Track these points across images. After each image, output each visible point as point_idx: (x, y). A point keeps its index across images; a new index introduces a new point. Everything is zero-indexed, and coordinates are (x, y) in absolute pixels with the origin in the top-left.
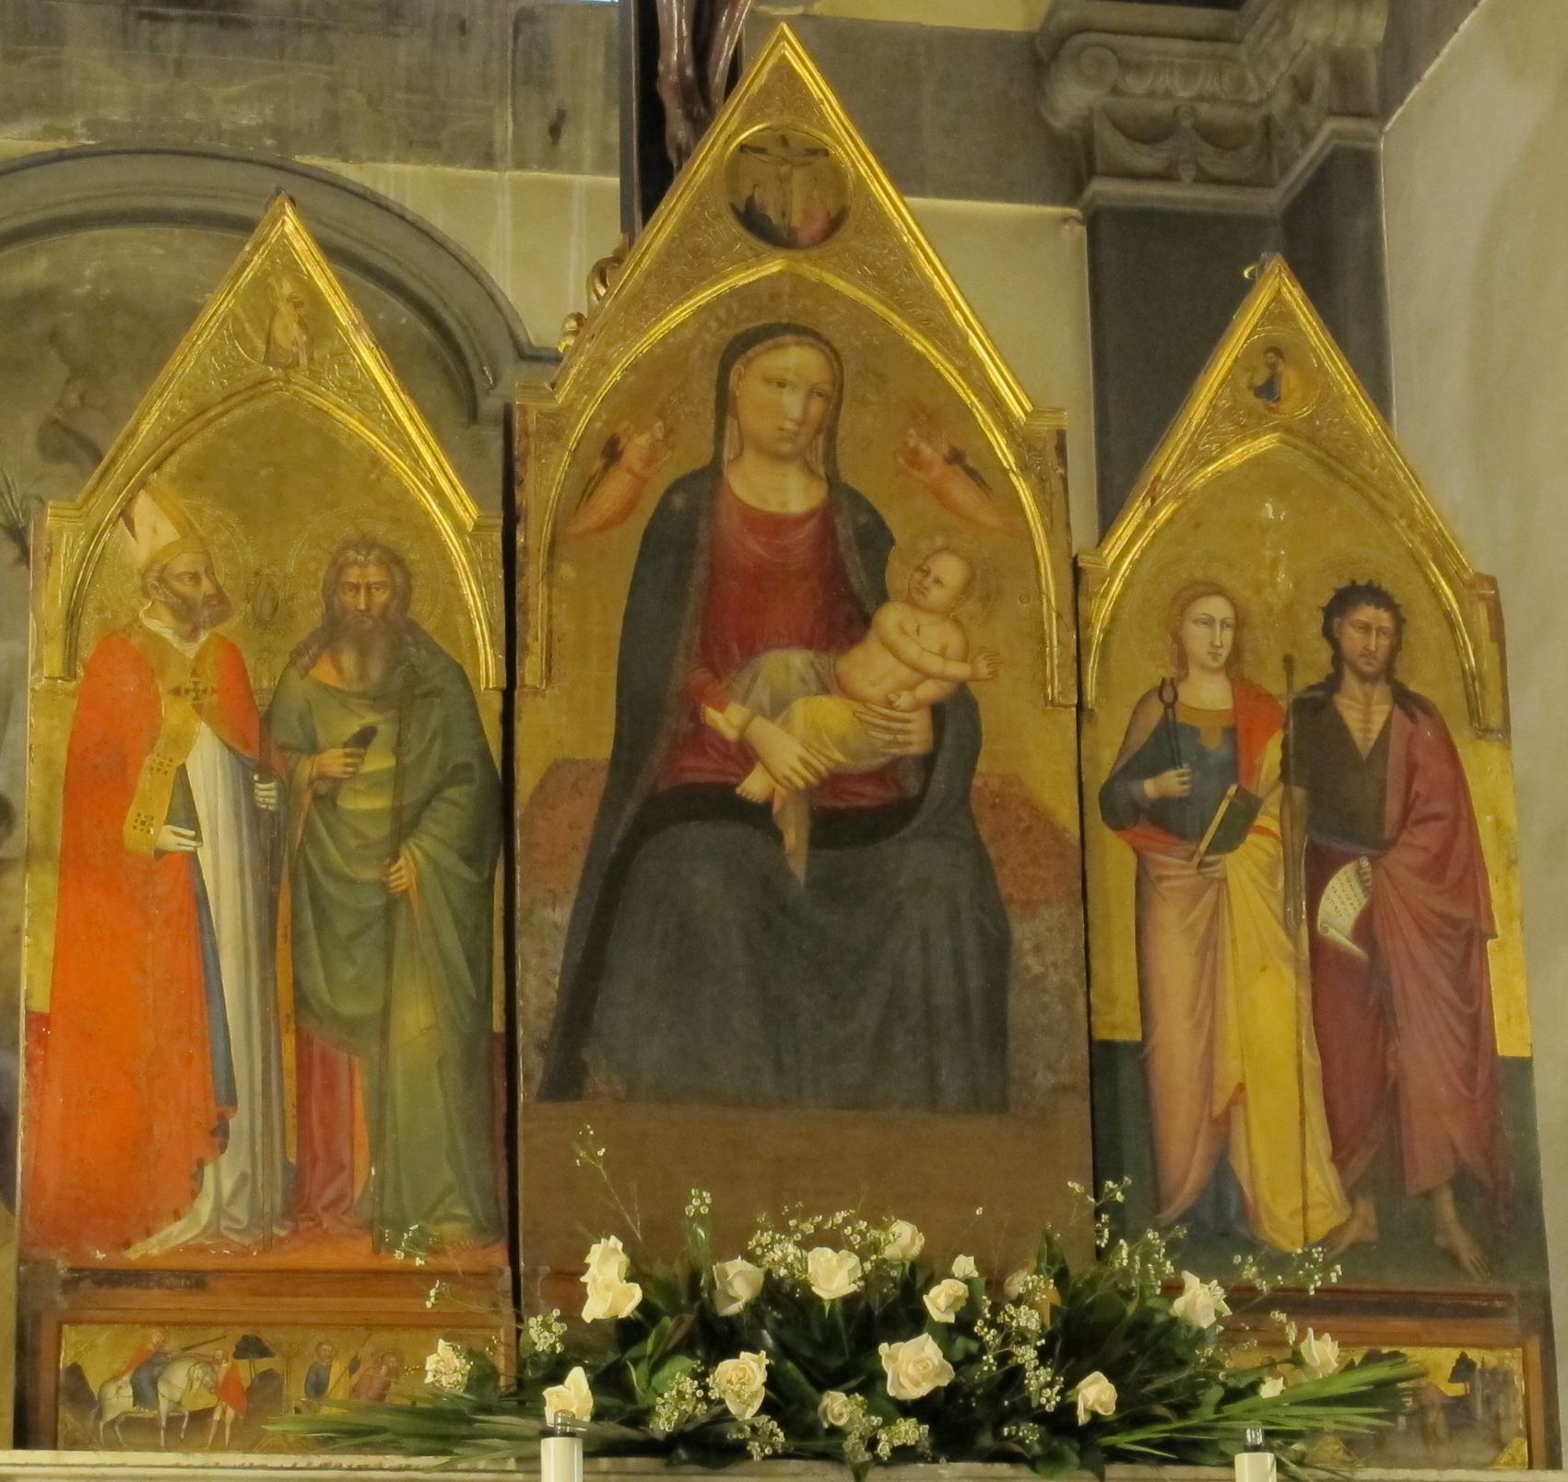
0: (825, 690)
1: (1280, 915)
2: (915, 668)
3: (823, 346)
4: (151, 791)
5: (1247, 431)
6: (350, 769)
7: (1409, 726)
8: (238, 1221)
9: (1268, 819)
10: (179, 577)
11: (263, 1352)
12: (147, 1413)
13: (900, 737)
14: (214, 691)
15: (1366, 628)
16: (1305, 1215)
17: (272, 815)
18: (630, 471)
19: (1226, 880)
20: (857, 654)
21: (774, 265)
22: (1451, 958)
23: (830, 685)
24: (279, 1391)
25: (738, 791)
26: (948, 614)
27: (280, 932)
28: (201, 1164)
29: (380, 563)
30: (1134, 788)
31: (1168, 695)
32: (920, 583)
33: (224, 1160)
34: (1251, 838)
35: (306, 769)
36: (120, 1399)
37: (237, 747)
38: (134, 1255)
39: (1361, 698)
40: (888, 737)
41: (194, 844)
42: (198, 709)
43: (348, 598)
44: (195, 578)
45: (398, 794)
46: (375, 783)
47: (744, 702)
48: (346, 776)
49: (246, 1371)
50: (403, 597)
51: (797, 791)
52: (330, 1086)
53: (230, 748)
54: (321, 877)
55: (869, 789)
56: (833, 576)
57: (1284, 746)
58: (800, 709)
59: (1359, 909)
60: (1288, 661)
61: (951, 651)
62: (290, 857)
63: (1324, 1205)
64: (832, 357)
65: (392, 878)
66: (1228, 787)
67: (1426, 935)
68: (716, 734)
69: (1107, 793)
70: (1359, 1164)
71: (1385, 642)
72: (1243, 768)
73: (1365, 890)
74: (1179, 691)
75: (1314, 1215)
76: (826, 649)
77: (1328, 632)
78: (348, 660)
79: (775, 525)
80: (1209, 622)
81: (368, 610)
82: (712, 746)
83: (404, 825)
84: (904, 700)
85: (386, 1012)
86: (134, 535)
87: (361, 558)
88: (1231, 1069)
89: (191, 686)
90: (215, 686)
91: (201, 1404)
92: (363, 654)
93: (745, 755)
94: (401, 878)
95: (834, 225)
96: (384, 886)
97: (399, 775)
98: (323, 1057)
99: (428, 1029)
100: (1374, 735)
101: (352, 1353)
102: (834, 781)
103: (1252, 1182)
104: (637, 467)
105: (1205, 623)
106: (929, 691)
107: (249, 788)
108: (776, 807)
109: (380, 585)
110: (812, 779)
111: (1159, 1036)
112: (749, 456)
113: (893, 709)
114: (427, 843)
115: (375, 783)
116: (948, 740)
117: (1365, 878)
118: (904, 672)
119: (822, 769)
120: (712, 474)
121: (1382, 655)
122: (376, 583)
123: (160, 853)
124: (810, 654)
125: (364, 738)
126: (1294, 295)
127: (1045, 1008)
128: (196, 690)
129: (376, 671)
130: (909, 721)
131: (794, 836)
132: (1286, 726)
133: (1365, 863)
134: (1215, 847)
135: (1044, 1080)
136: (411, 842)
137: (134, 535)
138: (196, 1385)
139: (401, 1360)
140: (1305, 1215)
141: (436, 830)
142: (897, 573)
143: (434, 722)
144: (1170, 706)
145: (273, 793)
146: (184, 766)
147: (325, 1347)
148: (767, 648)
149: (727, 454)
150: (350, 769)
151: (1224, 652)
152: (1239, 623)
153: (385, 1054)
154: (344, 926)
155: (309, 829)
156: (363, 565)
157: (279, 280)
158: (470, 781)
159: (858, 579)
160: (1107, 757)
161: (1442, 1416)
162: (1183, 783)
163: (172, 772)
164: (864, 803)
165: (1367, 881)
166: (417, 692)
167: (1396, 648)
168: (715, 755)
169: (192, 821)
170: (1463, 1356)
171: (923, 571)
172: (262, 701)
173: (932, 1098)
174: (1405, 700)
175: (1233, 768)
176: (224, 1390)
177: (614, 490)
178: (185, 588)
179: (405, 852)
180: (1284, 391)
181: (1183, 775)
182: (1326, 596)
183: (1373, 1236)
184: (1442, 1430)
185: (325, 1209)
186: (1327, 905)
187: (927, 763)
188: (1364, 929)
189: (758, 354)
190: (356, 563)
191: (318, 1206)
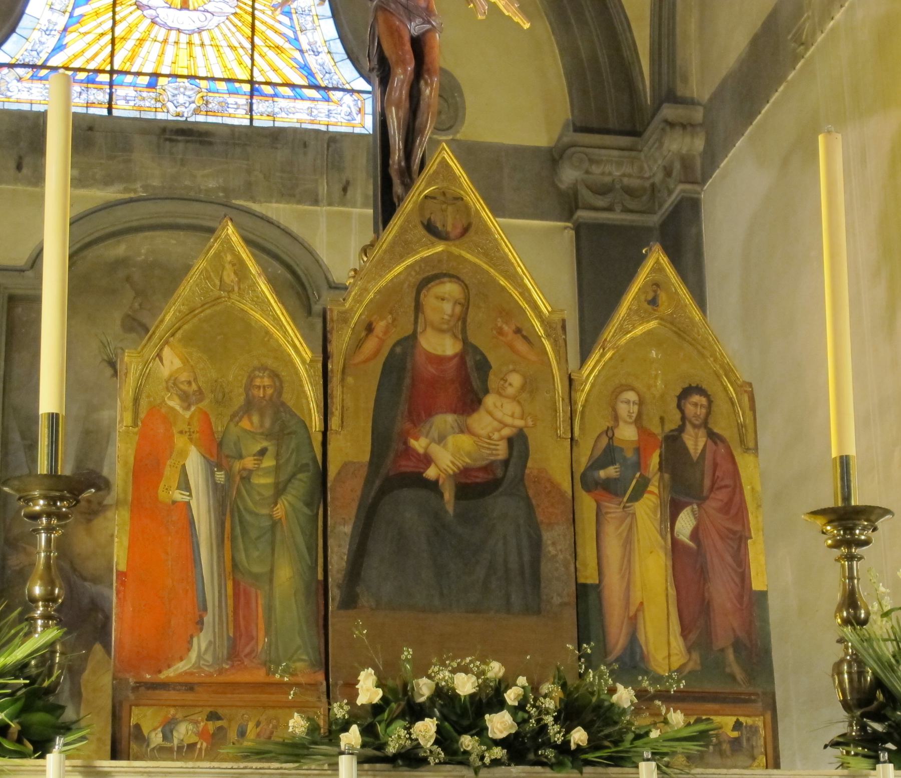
0: (462, 432)
1: (659, 529)
2: (500, 422)
3: (460, 283)
4: (170, 475)
5: (644, 320)
6: (256, 466)
7: (714, 447)
8: (207, 661)
9: (653, 487)
10: (182, 383)
11: (218, 717)
12: (168, 745)
13: (494, 452)
14: (197, 432)
15: (696, 405)
16: (669, 659)
17: (223, 486)
18: (377, 337)
20: (476, 416)
21: (440, 248)
22: (733, 548)
23: (464, 429)
24: (225, 736)
25: (424, 475)
26: (514, 399)
27: (226, 536)
28: (192, 637)
29: (269, 377)
30: (595, 474)
31: (610, 434)
33: (202, 635)
34: (646, 495)
35: (237, 466)
36: (157, 739)
37: (207, 456)
38: (163, 676)
39: (693, 435)
40: (488, 452)
41: (188, 498)
42: (191, 440)
43: (255, 392)
44: (189, 383)
45: (277, 476)
46: (267, 472)
47: (427, 436)
49: (211, 726)
50: (279, 391)
51: (450, 476)
52: (248, 603)
53: (204, 457)
54: (244, 513)
55: (481, 475)
56: (465, 382)
57: (660, 456)
58: (450, 440)
59: (693, 526)
60: (662, 419)
62: (230, 504)
63: (677, 654)
64: (465, 287)
65: (275, 513)
66: (636, 474)
67: (721, 538)
68: (414, 450)
69: (583, 476)
70: (693, 637)
71: (704, 411)
72: (642, 465)
73: (695, 518)
74: (615, 432)
75: (673, 659)
76: (462, 414)
77: (679, 407)
78: (256, 419)
79: (440, 360)
80: (628, 402)
81: (264, 397)
82: (412, 456)
83: (280, 490)
84: (496, 436)
85: (272, 571)
86: (163, 364)
87: (261, 374)
88: (637, 596)
89: (187, 430)
90: (198, 430)
91: (192, 741)
92: (262, 416)
93: (427, 460)
94: (278, 513)
95: (466, 230)
96: (271, 516)
97: (277, 468)
98: (245, 590)
100: (699, 451)
101: (257, 719)
102: (466, 471)
103: (647, 645)
104: (381, 335)
106: (506, 432)
107: (213, 474)
108: (441, 482)
109: (269, 386)
110: (456, 470)
111: (606, 581)
112: (429, 330)
114: (290, 498)
115: (267, 472)
116: (515, 453)
118: (496, 424)
119: (460, 465)
120: (412, 338)
121: (702, 416)
123: (174, 502)
124: (455, 416)
125: (263, 452)
126: (664, 260)
127: (557, 569)
128: (189, 432)
129: (267, 423)
130: (498, 445)
131: (448, 495)
132: (661, 447)
133: (695, 507)
135: (556, 600)
136: (283, 497)
137: (163, 364)
138: (190, 732)
139: (278, 721)
140: (669, 659)
141: (294, 492)
142: (493, 381)
143: (293, 445)
144: (611, 438)
145: (223, 476)
146: (184, 464)
147: (245, 716)
148: (437, 414)
149: (419, 330)
150: (256, 466)
151: (634, 415)
152: (641, 403)
153: (271, 589)
154: (253, 534)
155: (239, 491)
156: (262, 378)
157: (225, 254)
158: (308, 471)
159: (476, 384)
160: (583, 461)
161: (728, 746)
163: (179, 467)
164: (478, 480)
165: (696, 514)
166: (285, 432)
167: (708, 414)
169: (188, 488)
170: (738, 720)
172: (218, 436)
173: (508, 607)
174: (712, 436)
175: (638, 465)
176: (202, 734)
177: (370, 345)
178: (185, 387)
179: (280, 502)
180: (660, 302)
181: (616, 468)
182: (679, 391)
183: (698, 668)
184: (728, 753)
185: (246, 656)
187: (506, 463)
188: (695, 535)
189: (433, 286)
190: (258, 376)
191: (242, 655)
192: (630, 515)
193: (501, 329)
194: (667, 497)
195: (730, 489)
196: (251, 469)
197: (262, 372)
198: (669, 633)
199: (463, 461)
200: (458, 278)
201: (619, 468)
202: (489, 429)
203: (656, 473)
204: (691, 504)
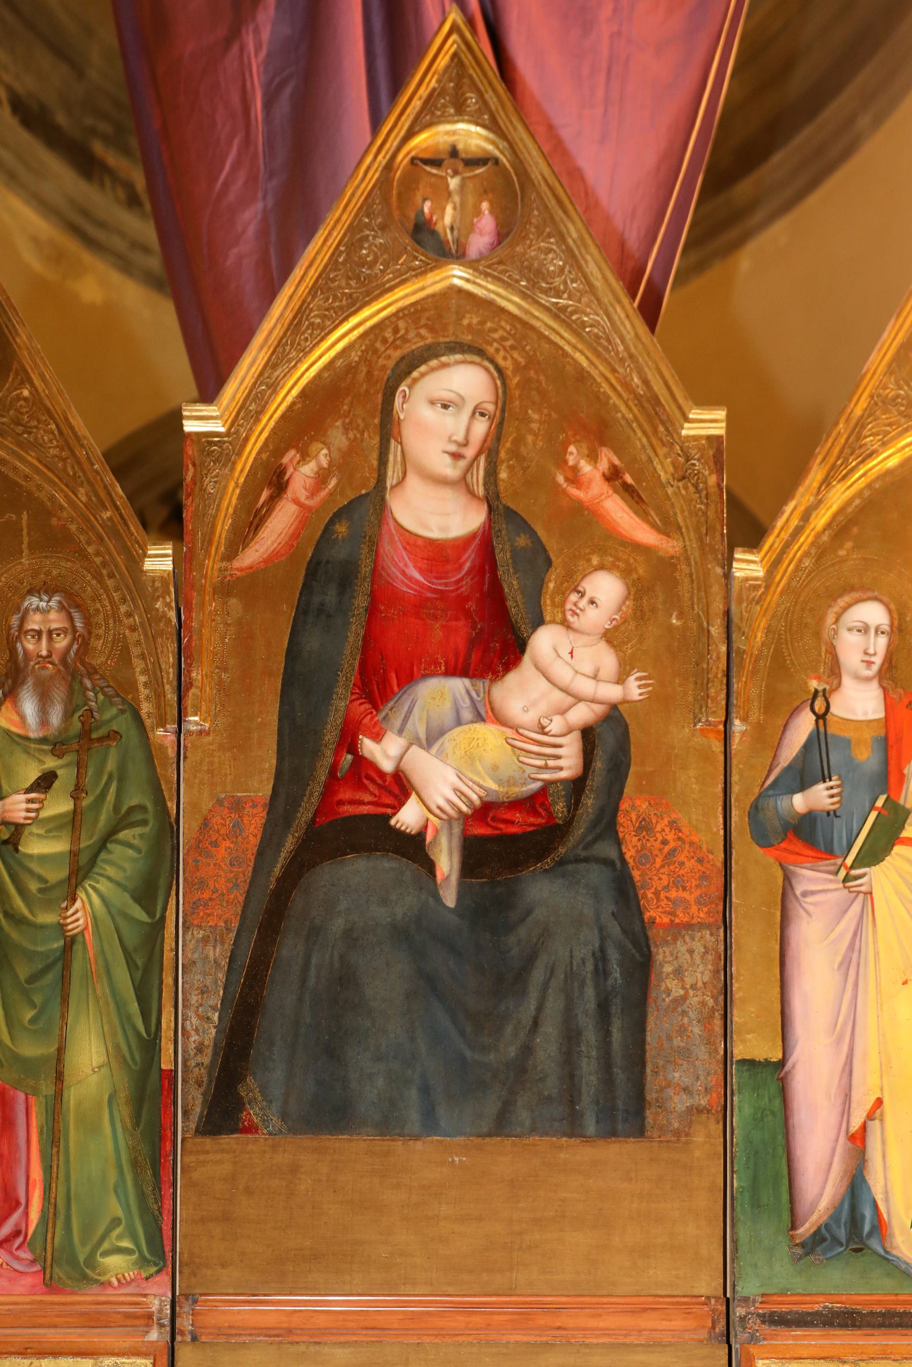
0: (480, 718)
2: (565, 691)
6: (33, 815)
13: (551, 763)
18: (296, 502)
19: (871, 893)
20: (512, 678)
25: (393, 822)
29: (62, 607)
31: (819, 705)
32: (575, 604)
34: (897, 849)
45: (75, 839)
46: (55, 825)
47: (400, 732)
48: (29, 821)
51: (450, 820)
55: (518, 817)
61: (602, 674)
64: (496, 374)
65: (69, 920)
68: (372, 765)
69: (755, 810)
72: (893, 779)
74: (831, 701)
78: (29, 706)
80: (864, 629)
81: (50, 655)
84: (556, 725)
85: (61, 1051)
87: (43, 604)
94: (77, 920)
96: (61, 927)
99: (99, 1067)
104: (302, 496)
105: (859, 631)
106: (582, 714)
108: (429, 838)
109: (64, 631)
110: (464, 809)
112: (413, 482)
113: (546, 734)
114: (104, 886)
115: (55, 825)
116: (599, 765)
118: (557, 696)
119: (474, 797)
122: (56, 629)
124: (467, 681)
125: (45, 782)
127: (682, 1030)
129: (56, 717)
130: (560, 746)
134: (859, 862)
135: (679, 1103)
141: (111, 871)
143: (111, 765)
144: (821, 717)
148: (425, 676)
149: (391, 478)
150: (33, 815)
151: (878, 660)
153: (59, 1095)
158: (144, 823)
159: (516, 604)
162: (832, 796)
164: (513, 830)
166: (94, 736)
168: (371, 787)
171: (579, 592)
179: (81, 894)
181: (832, 788)
187: (577, 786)
189: (423, 375)
190: (37, 609)
192: (861, 896)
193: (575, 469)
196: (22, 821)
197: (46, 598)
199: (480, 786)
200: (480, 352)
201: (838, 786)
202: (543, 707)
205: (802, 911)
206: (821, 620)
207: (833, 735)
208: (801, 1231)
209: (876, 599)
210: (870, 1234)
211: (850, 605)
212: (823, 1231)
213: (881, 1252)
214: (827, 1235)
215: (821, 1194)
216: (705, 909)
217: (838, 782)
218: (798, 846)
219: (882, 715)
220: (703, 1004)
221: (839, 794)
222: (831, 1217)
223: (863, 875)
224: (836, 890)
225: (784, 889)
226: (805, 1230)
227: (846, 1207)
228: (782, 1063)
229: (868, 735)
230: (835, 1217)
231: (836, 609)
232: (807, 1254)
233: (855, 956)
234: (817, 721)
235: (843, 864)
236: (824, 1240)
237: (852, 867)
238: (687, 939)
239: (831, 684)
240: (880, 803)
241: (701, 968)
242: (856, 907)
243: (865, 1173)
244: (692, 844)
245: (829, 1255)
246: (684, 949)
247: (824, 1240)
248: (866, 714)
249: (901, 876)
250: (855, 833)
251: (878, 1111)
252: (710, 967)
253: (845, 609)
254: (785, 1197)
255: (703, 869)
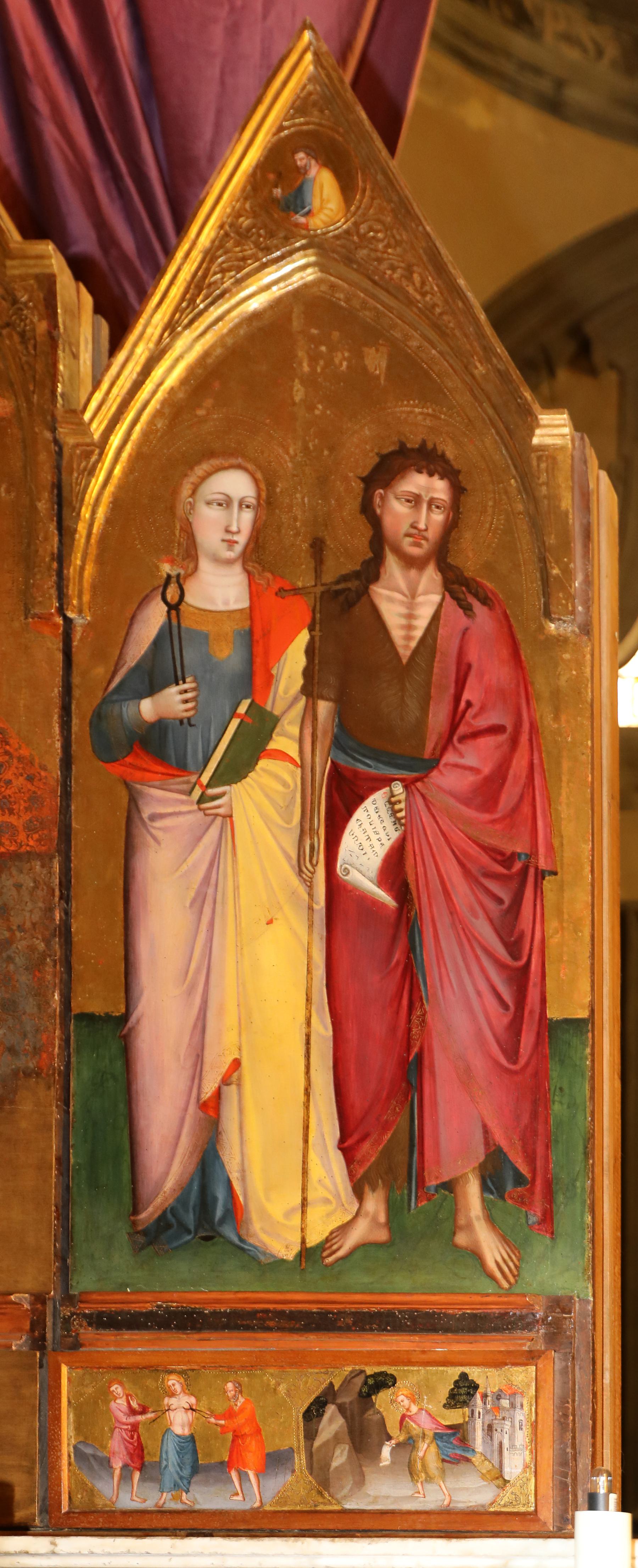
1: (294, 855)
7: (464, 621)
15: (415, 500)
16: (303, 1212)
19: (231, 816)
22: (500, 901)
30: (128, 710)
31: (172, 593)
34: (263, 763)
57: (310, 651)
59: (388, 844)
60: (318, 547)
63: (327, 1201)
66: (238, 704)
67: (467, 873)
70: (370, 1152)
71: (438, 517)
72: (259, 681)
74: (185, 587)
75: (314, 1213)
80: (226, 503)
100: (418, 634)
103: (243, 1179)
105: (220, 505)
117: (397, 807)
121: (433, 534)
132: (311, 630)
133: (398, 788)
134: (218, 779)
140: (303, 1212)
144: (174, 608)
151: (242, 539)
162: (186, 701)
165: (401, 810)
167: (451, 527)
170: (464, 1376)
181: (186, 691)
183: (382, 1235)
184: (433, 1463)
186: (348, 843)
192: (219, 820)
194: (323, 768)
195: (502, 738)
198: (306, 1141)
201: (194, 689)
203: (295, 700)
204: (387, 781)
205: (149, 838)
206: (175, 492)
207: (188, 629)
208: (143, 1216)
209: (239, 467)
210: (223, 1221)
211: (209, 474)
212: (169, 1216)
213: (236, 1240)
214: (173, 1221)
215: (167, 1173)
216: (36, 836)
217: (193, 685)
218: (146, 762)
219: (246, 604)
220: (32, 948)
221: (194, 699)
222: (178, 1200)
223: (223, 794)
224: (189, 812)
225: (129, 812)
226: (148, 1215)
227: (196, 1187)
228: (125, 1018)
229: (228, 627)
230: (182, 1199)
231: (193, 479)
232: (150, 1243)
233: (210, 891)
234: (169, 612)
235: (198, 782)
236: (169, 1226)
237: (209, 785)
238: (14, 872)
239: (186, 569)
240: (242, 709)
241: (30, 906)
242: (214, 832)
243: (218, 1147)
244: (20, 759)
245: (175, 1244)
246: (9, 883)
247: (169, 1226)
248: (226, 603)
249: (267, 796)
250: (212, 745)
251: (235, 1075)
252: (41, 904)
253: (203, 479)
254: (126, 1176)
255: (33, 788)
